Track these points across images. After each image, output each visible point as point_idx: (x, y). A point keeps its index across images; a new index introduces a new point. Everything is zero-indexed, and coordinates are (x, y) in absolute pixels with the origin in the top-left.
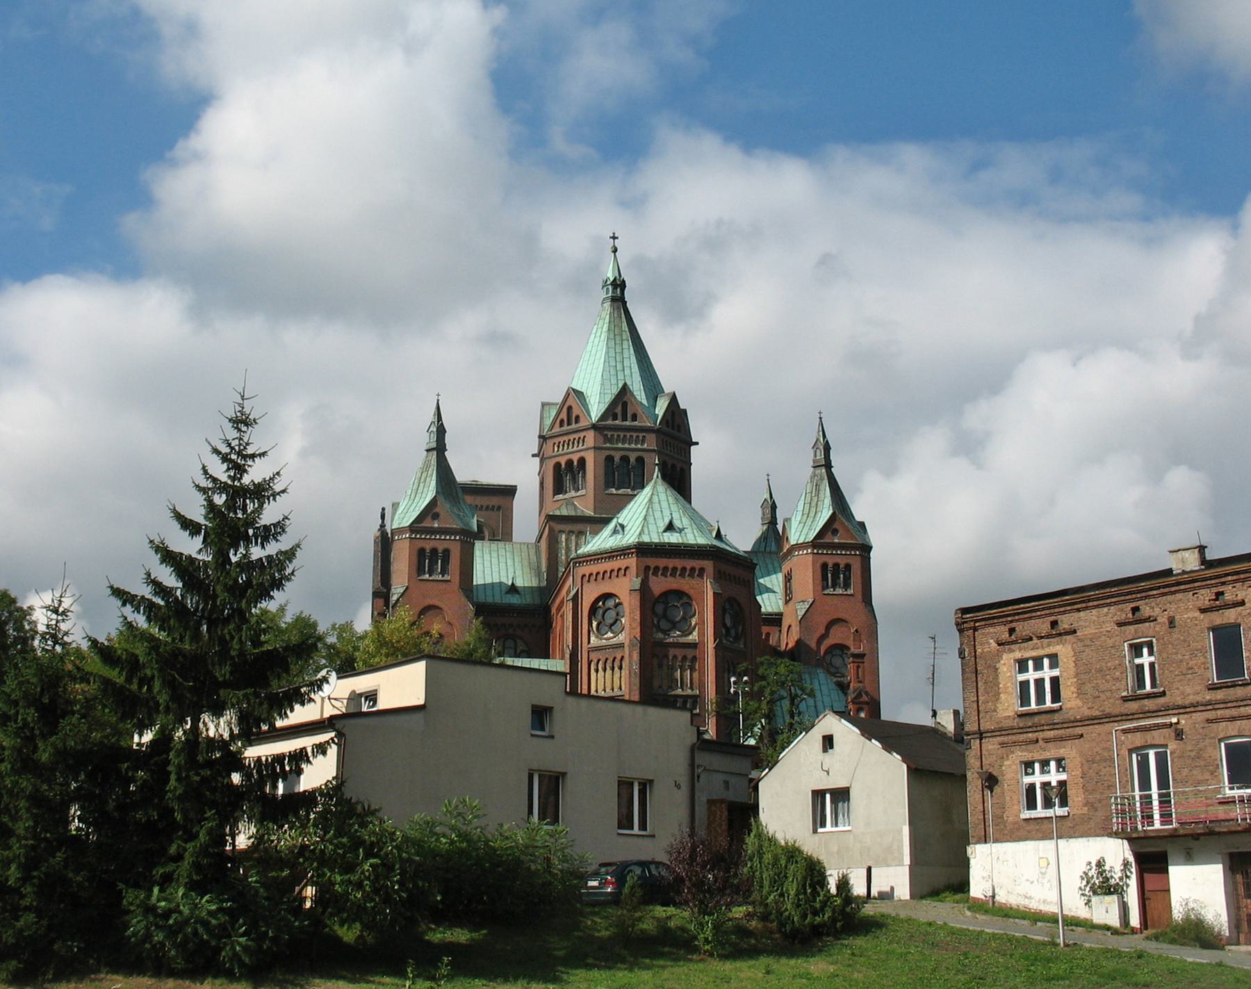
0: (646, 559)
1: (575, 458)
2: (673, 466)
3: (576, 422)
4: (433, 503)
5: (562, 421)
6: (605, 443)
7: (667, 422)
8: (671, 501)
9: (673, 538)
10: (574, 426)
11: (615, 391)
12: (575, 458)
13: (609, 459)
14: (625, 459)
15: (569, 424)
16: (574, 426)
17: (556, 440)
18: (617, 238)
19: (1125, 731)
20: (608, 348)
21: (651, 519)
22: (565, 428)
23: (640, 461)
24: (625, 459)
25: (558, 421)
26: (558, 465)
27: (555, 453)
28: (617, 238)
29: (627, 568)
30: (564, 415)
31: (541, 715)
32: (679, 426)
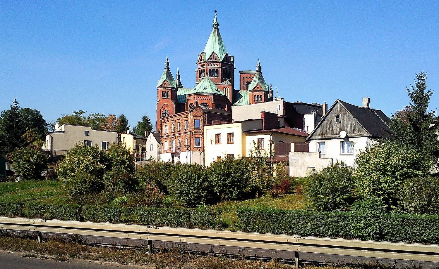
2: (227, 71)
4: (165, 81)
7: (225, 60)
8: (208, 83)
9: (205, 91)
10: (203, 61)
13: (210, 69)
14: (214, 69)
15: (202, 61)
19: (172, 137)
20: (212, 41)
21: (201, 87)
22: (201, 62)
23: (217, 70)
24: (214, 69)
27: (199, 68)
29: (195, 98)
30: (201, 59)
31: (86, 133)
32: (229, 61)
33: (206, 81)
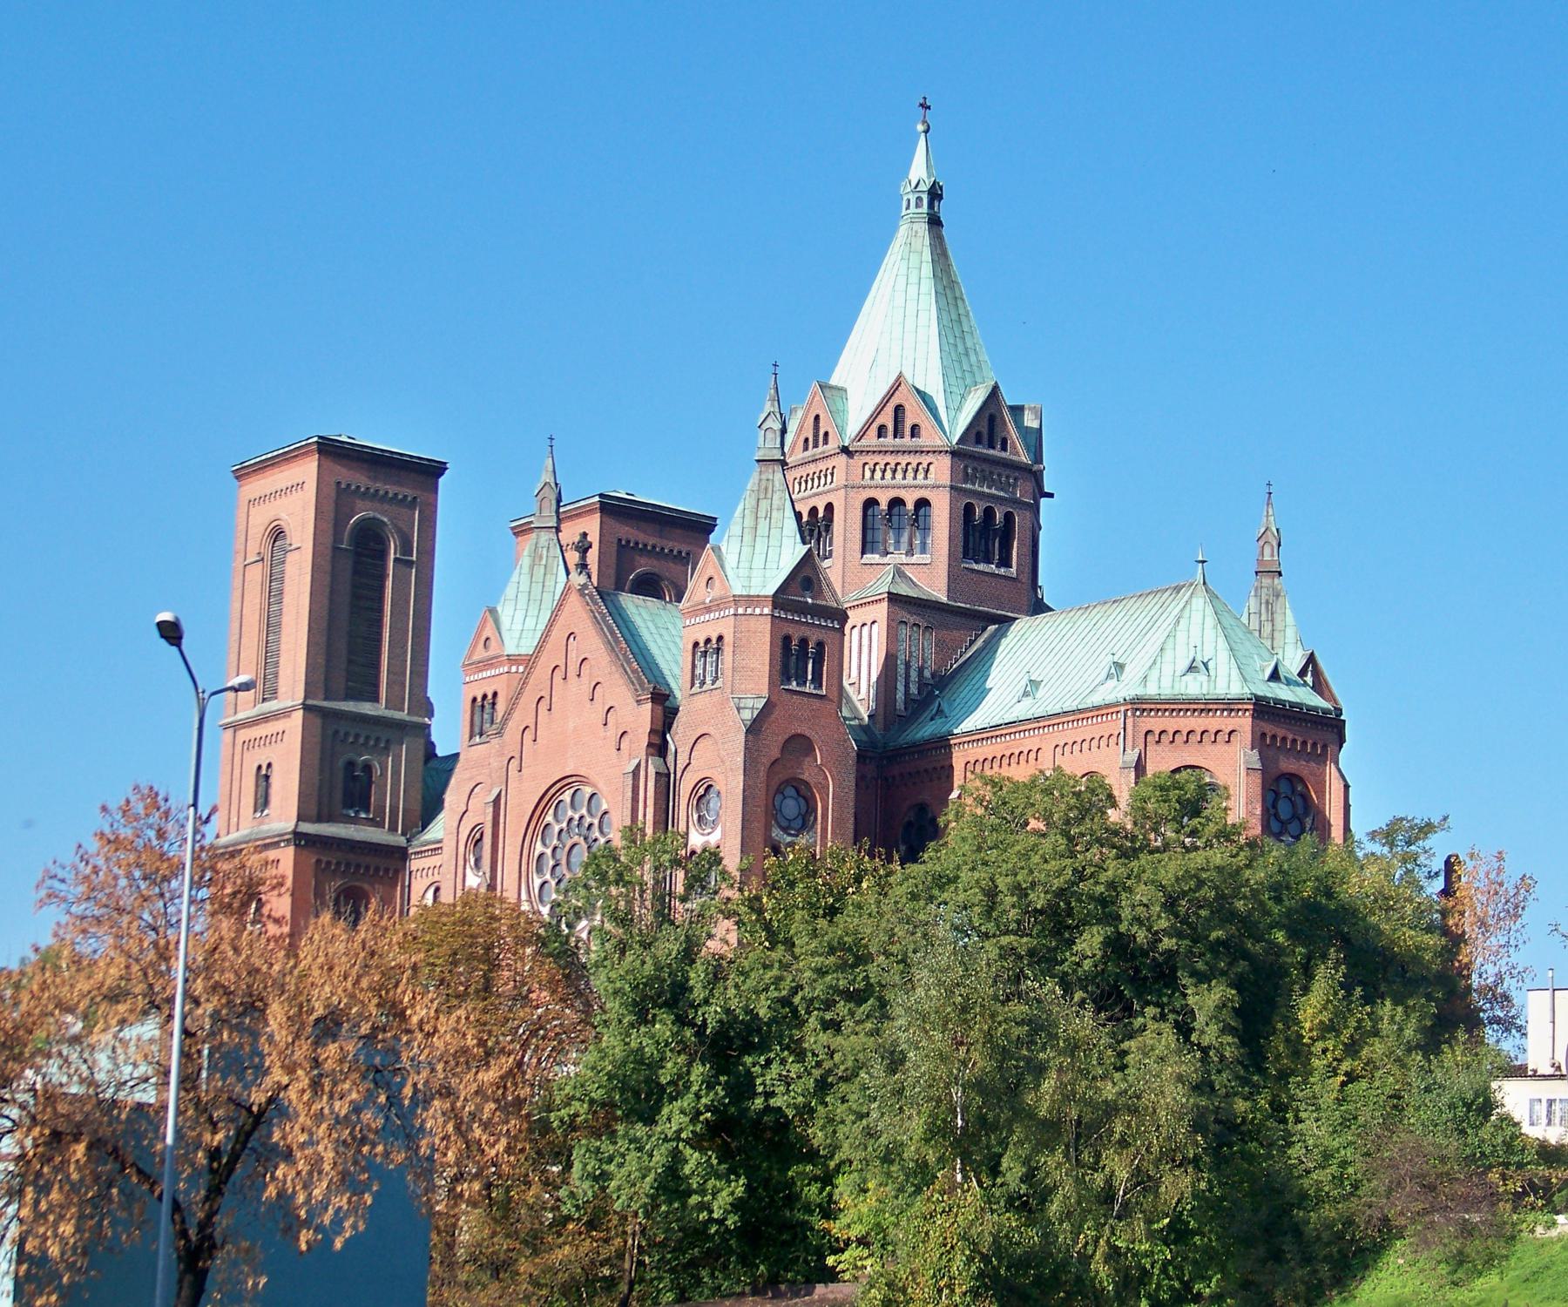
0: (1262, 724)
1: (910, 500)
3: (913, 436)
5: (881, 431)
6: (966, 483)
10: (907, 441)
11: (891, 381)
12: (910, 500)
16: (907, 441)
17: (871, 459)
18: (929, 108)
25: (875, 426)
26: (871, 503)
27: (867, 481)
28: (929, 108)
30: (887, 418)
33: (1197, 617)
